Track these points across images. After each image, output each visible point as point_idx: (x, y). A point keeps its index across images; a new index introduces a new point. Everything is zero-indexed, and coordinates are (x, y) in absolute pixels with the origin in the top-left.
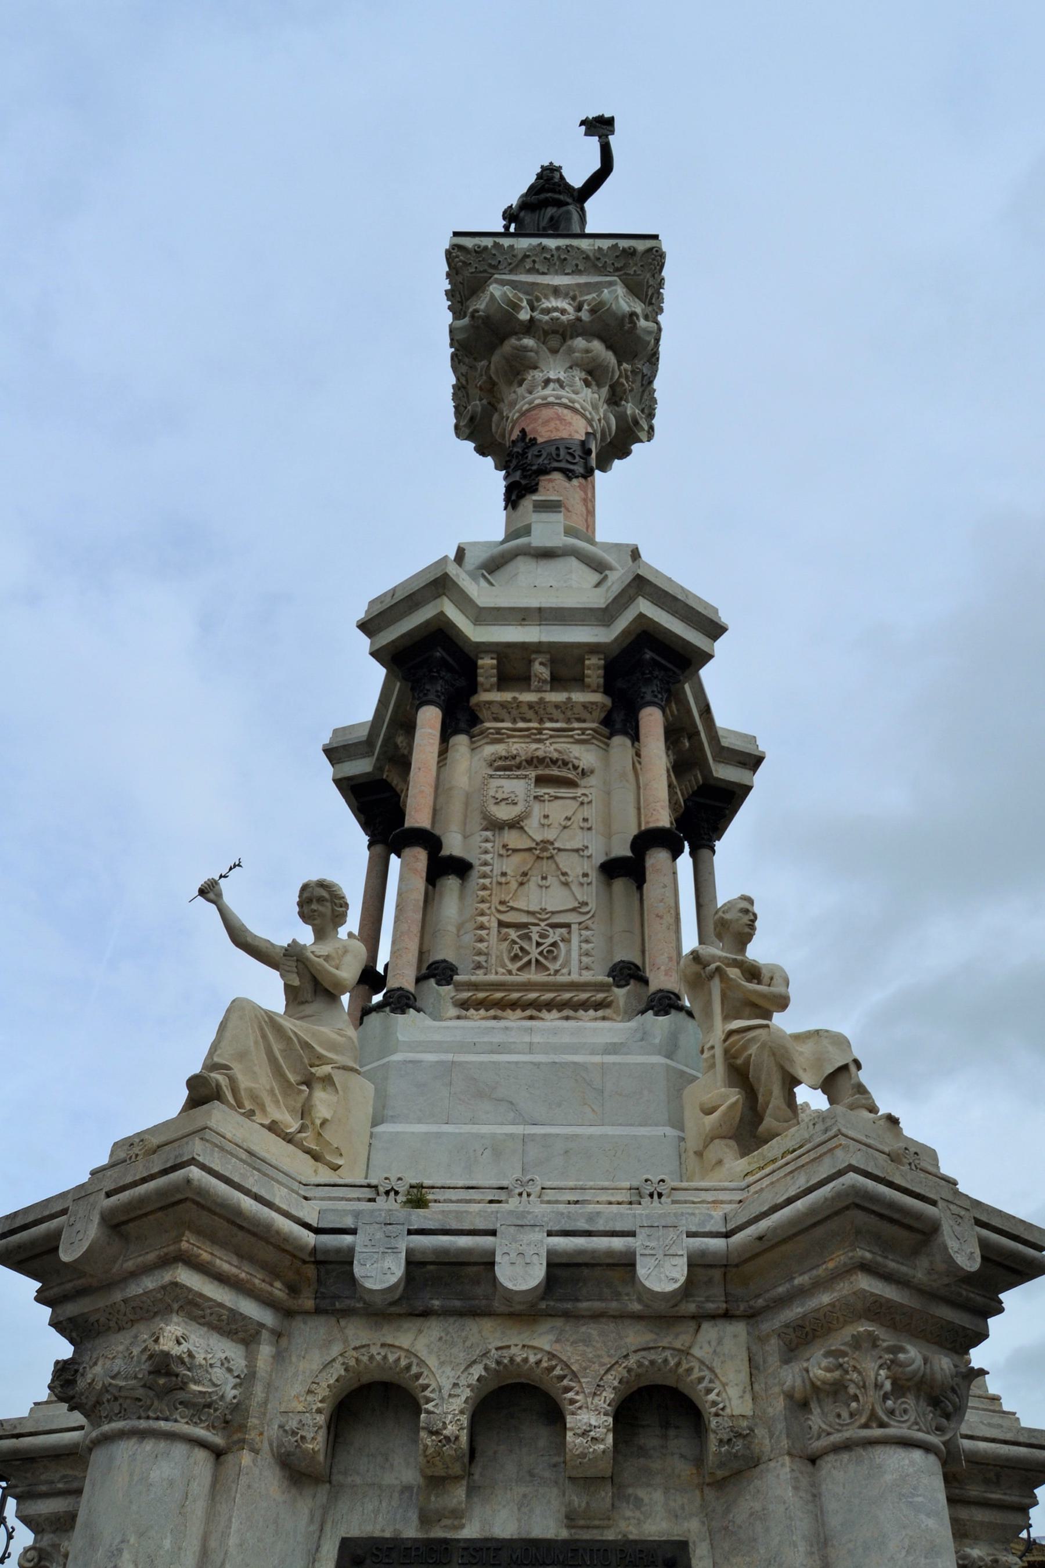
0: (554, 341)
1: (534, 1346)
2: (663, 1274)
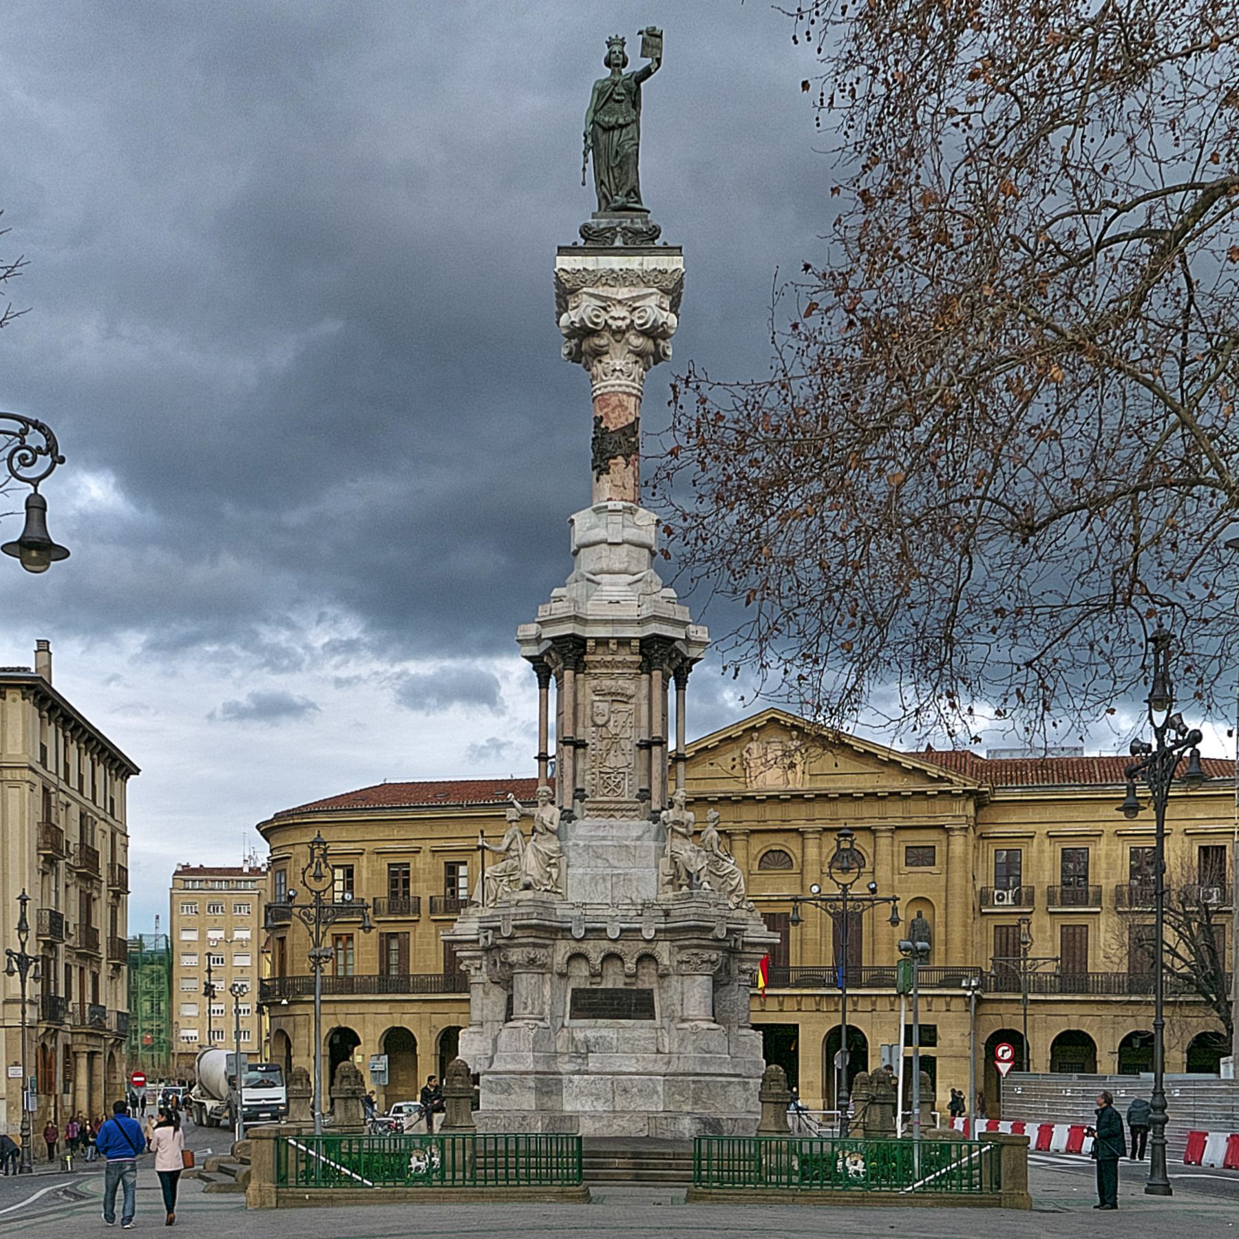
0: (618, 337)
1: (617, 948)
2: (649, 934)
